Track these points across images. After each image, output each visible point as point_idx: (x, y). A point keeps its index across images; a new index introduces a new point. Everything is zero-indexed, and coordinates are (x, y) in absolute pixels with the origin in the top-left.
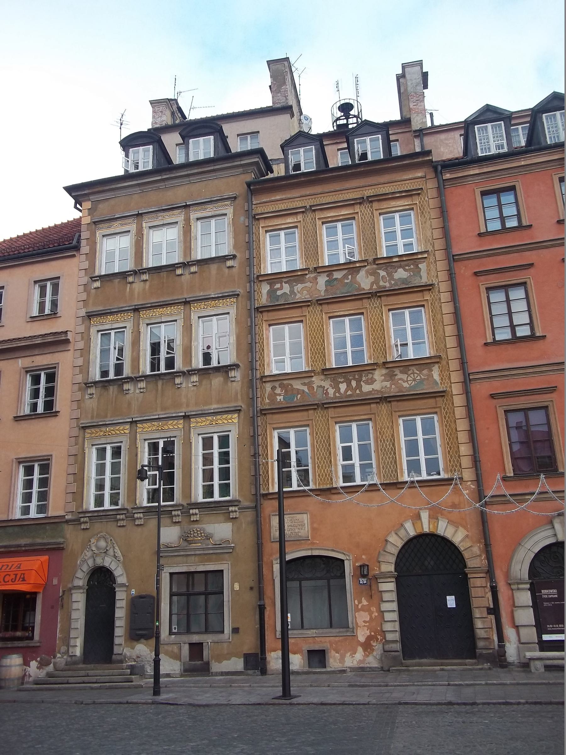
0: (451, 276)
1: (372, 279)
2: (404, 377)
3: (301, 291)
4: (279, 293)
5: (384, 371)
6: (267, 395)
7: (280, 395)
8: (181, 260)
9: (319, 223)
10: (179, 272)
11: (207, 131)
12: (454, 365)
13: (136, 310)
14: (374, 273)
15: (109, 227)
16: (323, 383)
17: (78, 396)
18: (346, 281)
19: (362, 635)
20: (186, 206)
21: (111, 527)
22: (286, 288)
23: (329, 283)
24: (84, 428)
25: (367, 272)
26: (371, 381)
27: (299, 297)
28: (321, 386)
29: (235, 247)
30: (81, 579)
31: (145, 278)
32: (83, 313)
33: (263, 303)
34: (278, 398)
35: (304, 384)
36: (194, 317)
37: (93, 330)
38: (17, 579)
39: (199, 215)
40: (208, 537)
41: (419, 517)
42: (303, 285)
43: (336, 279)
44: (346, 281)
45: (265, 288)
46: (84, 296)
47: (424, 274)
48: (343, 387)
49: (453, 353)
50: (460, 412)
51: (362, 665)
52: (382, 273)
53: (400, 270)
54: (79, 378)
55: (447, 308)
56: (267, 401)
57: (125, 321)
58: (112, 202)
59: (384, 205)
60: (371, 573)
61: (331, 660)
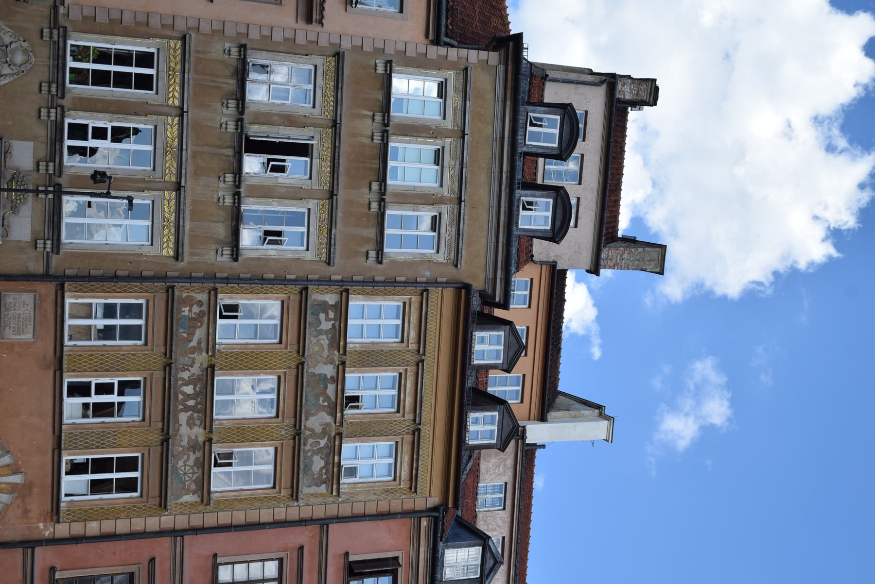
0: (302, 522)
1: (318, 430)
2: (191, 462)
3: (318, 344)
4: (322, 316)
5: (201, 439)
6: (192, 294)
7: (190, 311)
8: (389, 189)
9: (401, 370)
10: (375, 186)
11: (558, 223)
12: (196, 521)
13: (335, 124)
15: (456, 90)
16: (197, 366)
17: (230, 31)
18: (321, 399)
20: (460, 201)
21: (43, 73)
22: (326, 325)
23: (323, 379)
24: (183, 39)
25: (328, 425)
26: (190, 424)
27: (311, 340)
28: (193, 363)
29: (394, 263)
32: (346, 45)
33: (312, 298)
34: (187, 309)
35: (199, 343)
36: (312, 204)
37: (319, 60)
39: (445, 217)
40: (15, 209)
41: (16, 472)
42: (326, 347)
43: (326, 387)
44: (321, 399)
45: (331, 298)
46: (367, 48)
47: (314, 490)
48: (189, 390)
49: (210, 520)
50: (138, 524)
52: (323, 443)
53: (322, 463)
54: (254, 34)
55: (266, 516)
56: (185, 295)
57: (323, 107)
58: (489, 96)
59: (407, 448)
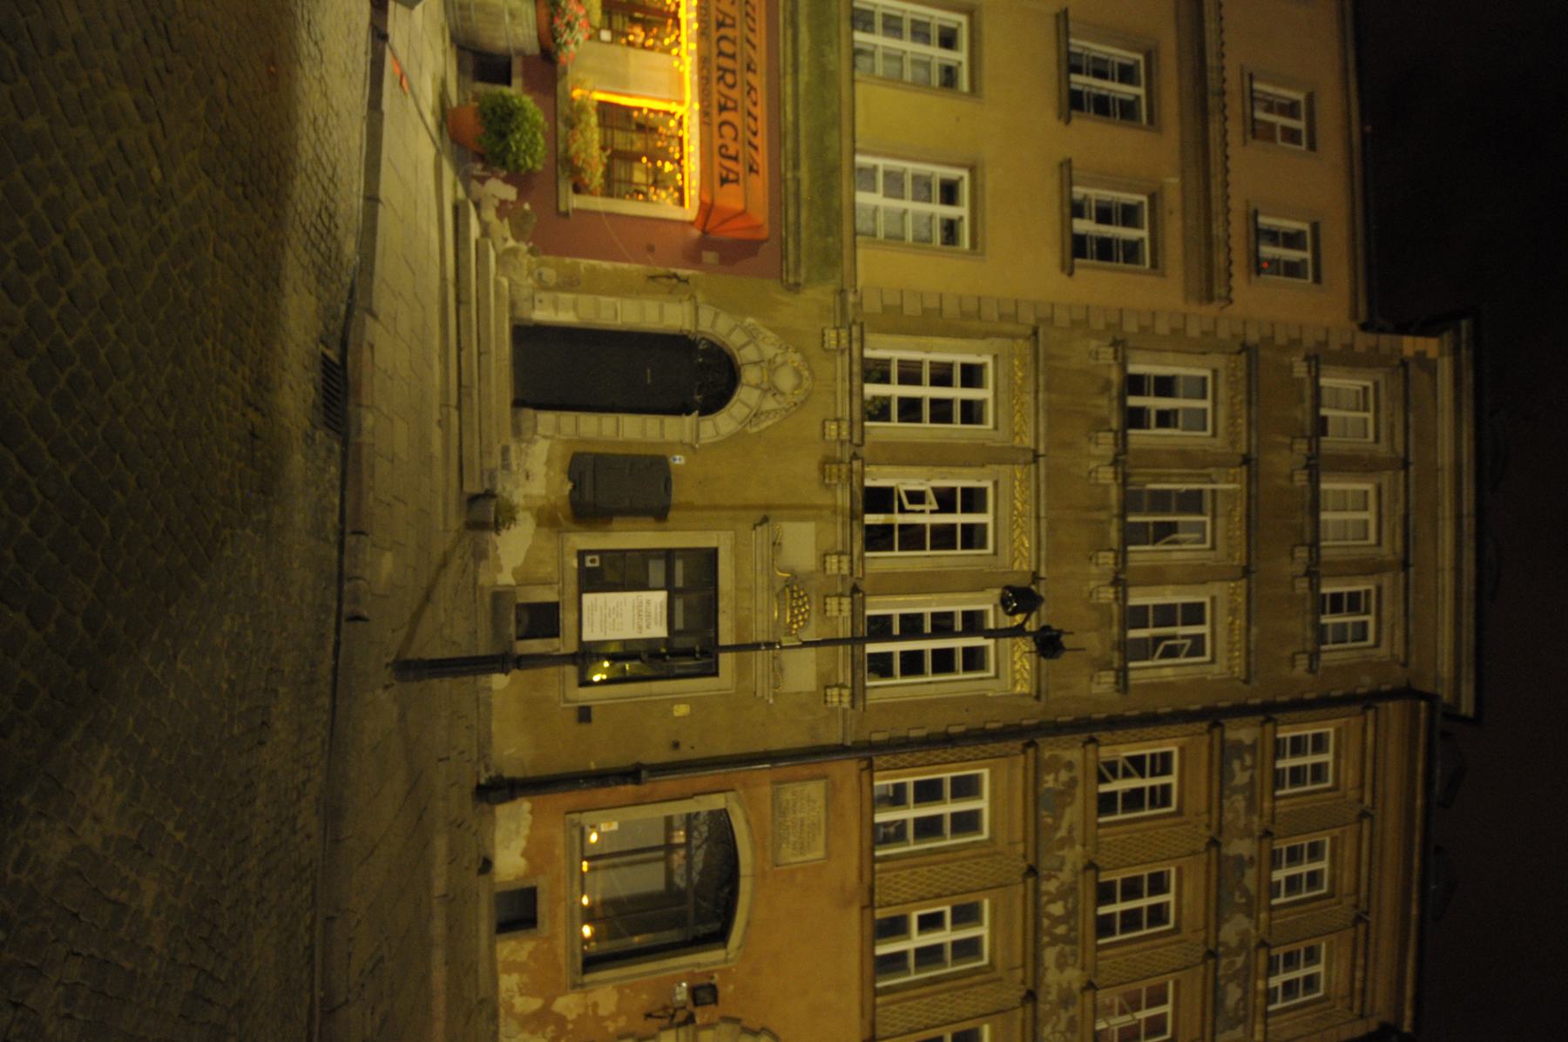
2: (1062, 1026)
5: (1076, 986)
7: (1056, 780)
14: (1243, 945)
16: (1068, 867)
19: (568, 1005)
20: (1406, 565)
22: (1241, 778)
26: (1061, 965)
28: (1063, 863)
30: (717, 325)
31: (1297, 478)
35: (1071, 830)
36: (1219, 589)
37: (1219, 361)
38: (729, 164)
43: (1243, 875)
44: (1237, 894)
46: (1281, 340)
51: (502, 1011)
52: (1240, 961)
60: (698, 1011)
61: (513, 943)
